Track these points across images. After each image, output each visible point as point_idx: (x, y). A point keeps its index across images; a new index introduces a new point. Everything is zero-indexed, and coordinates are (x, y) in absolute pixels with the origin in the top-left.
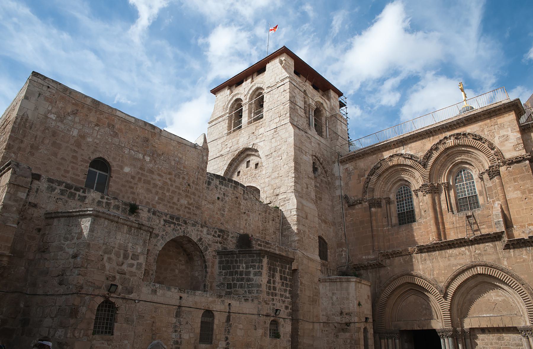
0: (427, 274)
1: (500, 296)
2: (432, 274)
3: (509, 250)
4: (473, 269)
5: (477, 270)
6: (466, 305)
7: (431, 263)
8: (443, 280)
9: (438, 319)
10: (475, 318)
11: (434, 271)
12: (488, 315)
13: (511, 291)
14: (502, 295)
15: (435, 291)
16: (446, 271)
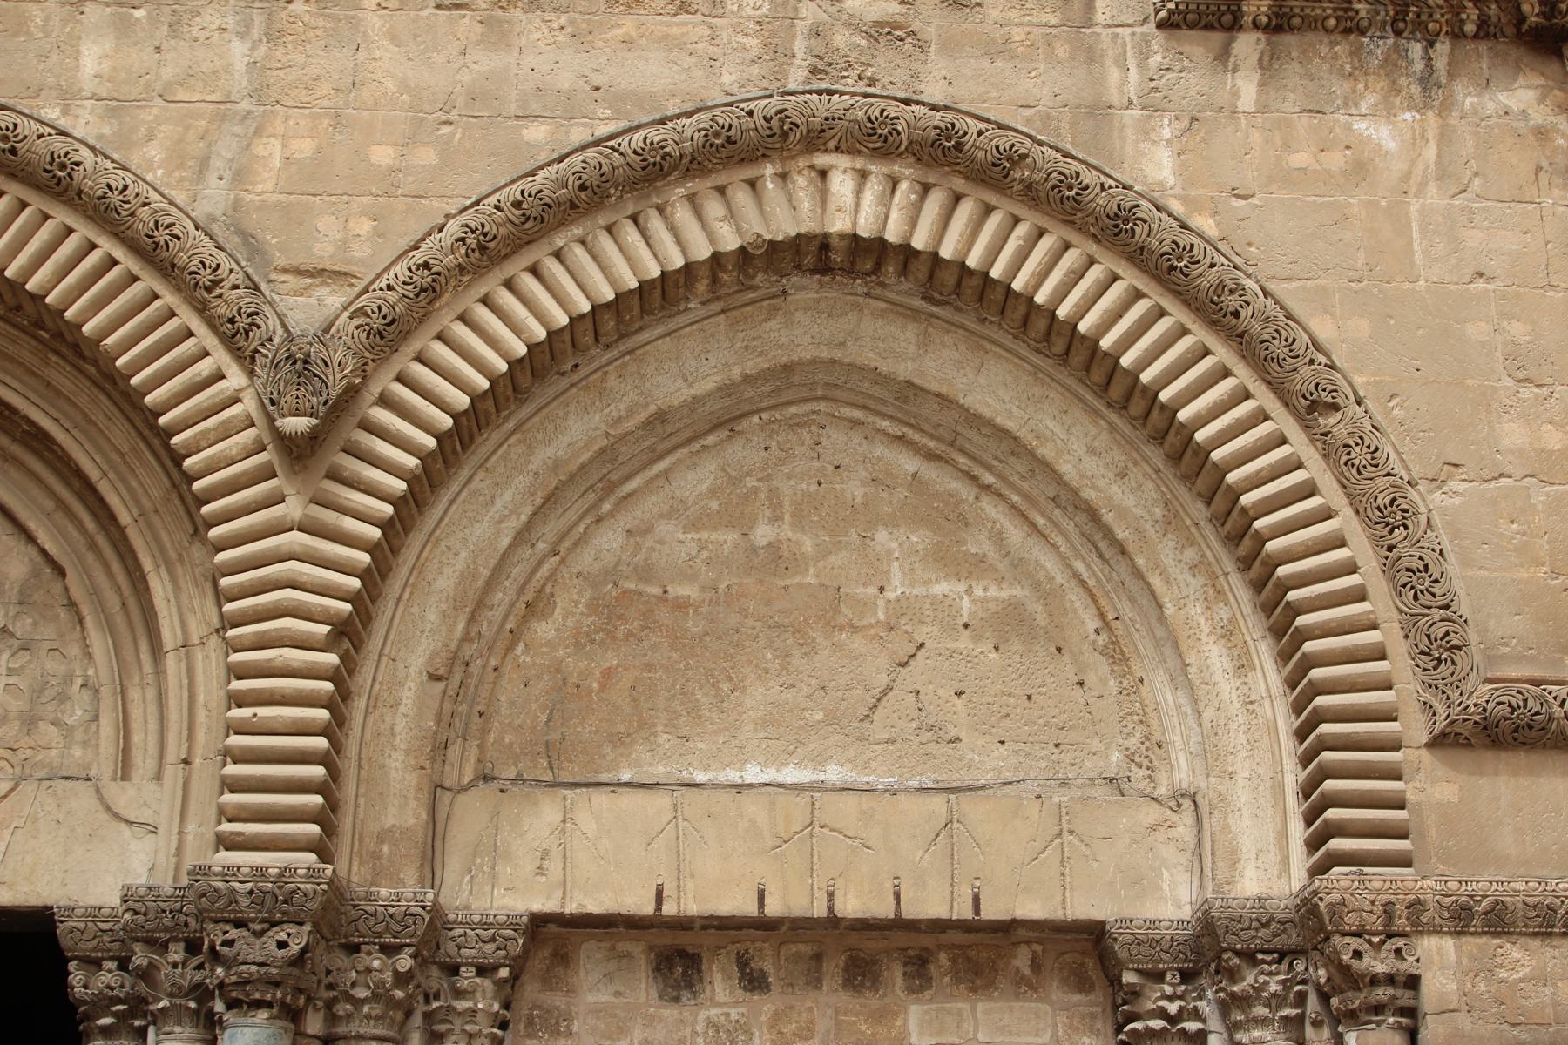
0: (155, 152)
1: (973, 567)
2: (217, 163)
3: (1217, 37)
4: (769, 170)
5: (823, 196)
6: (544, 630)
7: (242, 36)
8: (359, 251)
9: (125, 770)
10: (628, 799)
11: (258, 132)
12: (790, 775)
13: (1130, 501)
14: (993, 555)
15: (204, 367)
16: (426, 156)
